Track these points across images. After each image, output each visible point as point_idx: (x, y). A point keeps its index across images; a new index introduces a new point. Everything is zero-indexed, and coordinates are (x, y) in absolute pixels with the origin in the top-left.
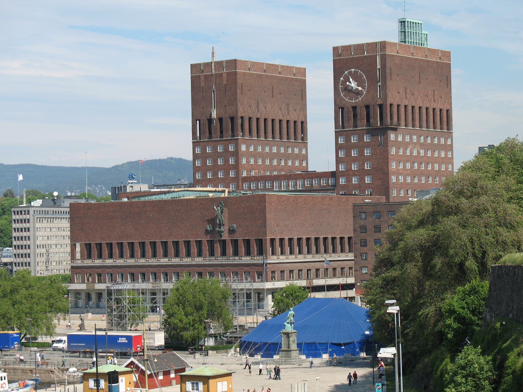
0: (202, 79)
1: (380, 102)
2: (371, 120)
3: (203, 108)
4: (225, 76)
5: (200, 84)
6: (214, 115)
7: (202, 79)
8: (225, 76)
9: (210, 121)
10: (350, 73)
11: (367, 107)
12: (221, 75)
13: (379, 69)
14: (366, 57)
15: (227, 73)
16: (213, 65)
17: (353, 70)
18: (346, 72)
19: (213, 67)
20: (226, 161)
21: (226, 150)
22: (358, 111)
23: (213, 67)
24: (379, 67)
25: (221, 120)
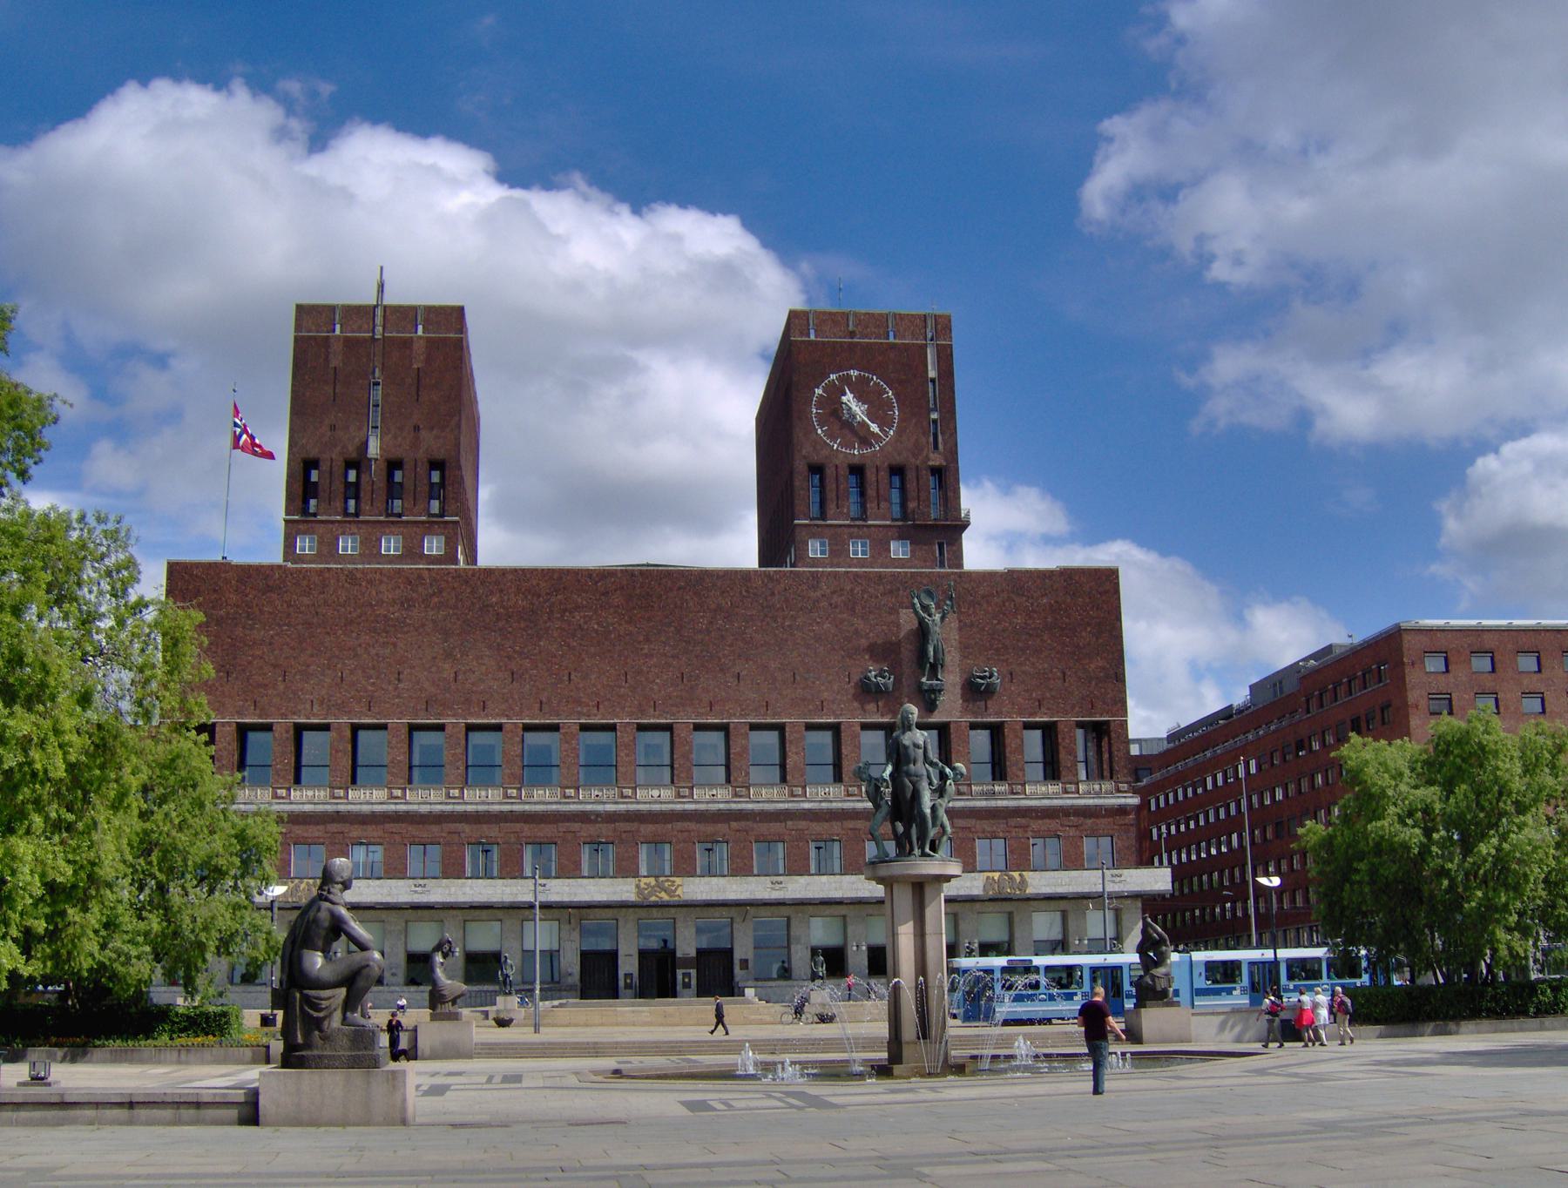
0: (337, 347)
1: (936, 460)
2: (912, 505)
3: (333, 428)
4: (419, 349)
5: (327, 359)
6: (374, 449)
7: (337, 347)
8: (419, 349)
12: (407, 344)
13: (933, 380)
14: (892, 346)
15: (429, 340)
16: (379, 312)
17: (854, 373)
18: (833, 377)
19: (379, 320)
22: (870, 476)
23: (379, 320)
24: (932, 374)
25: (393, 465)
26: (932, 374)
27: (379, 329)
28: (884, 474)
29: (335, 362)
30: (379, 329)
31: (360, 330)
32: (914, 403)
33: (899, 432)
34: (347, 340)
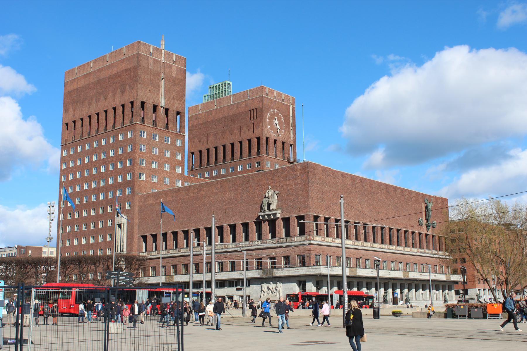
0: (151, 61)
4: (174, 68)
5: (148, 65)
6: (163, 103)
7: (151, 61)
9: (155, 108)
10: (274, 112)
11: (283, 143)
12: (170, 67)
16: (163, 52)
17: (276, 110)
19: (163, 55)
20: (173, 155)
21: (173, 144)
24: (291, 115)
25: (167, 111)
26: (291, 115)
27: (163, 59)
28: (281, 144)
29: (150, 68)
30: (163, 59)
31: (157, 57)
32: (287, 122)
33: (285, 131)
34: (154, 59)
